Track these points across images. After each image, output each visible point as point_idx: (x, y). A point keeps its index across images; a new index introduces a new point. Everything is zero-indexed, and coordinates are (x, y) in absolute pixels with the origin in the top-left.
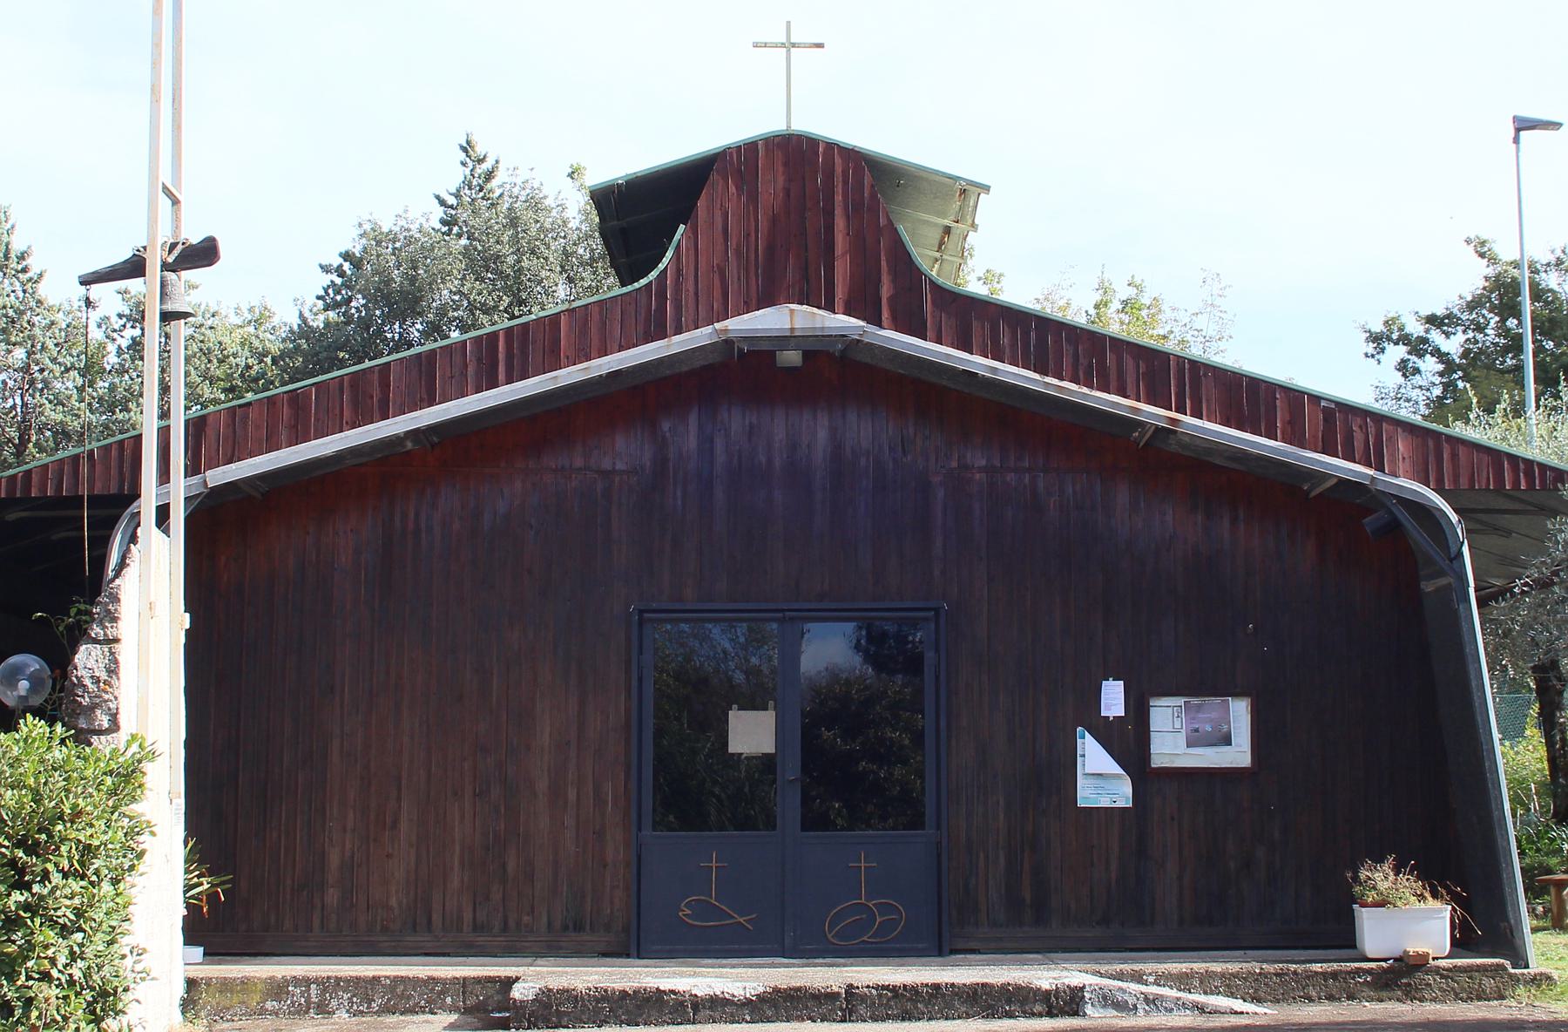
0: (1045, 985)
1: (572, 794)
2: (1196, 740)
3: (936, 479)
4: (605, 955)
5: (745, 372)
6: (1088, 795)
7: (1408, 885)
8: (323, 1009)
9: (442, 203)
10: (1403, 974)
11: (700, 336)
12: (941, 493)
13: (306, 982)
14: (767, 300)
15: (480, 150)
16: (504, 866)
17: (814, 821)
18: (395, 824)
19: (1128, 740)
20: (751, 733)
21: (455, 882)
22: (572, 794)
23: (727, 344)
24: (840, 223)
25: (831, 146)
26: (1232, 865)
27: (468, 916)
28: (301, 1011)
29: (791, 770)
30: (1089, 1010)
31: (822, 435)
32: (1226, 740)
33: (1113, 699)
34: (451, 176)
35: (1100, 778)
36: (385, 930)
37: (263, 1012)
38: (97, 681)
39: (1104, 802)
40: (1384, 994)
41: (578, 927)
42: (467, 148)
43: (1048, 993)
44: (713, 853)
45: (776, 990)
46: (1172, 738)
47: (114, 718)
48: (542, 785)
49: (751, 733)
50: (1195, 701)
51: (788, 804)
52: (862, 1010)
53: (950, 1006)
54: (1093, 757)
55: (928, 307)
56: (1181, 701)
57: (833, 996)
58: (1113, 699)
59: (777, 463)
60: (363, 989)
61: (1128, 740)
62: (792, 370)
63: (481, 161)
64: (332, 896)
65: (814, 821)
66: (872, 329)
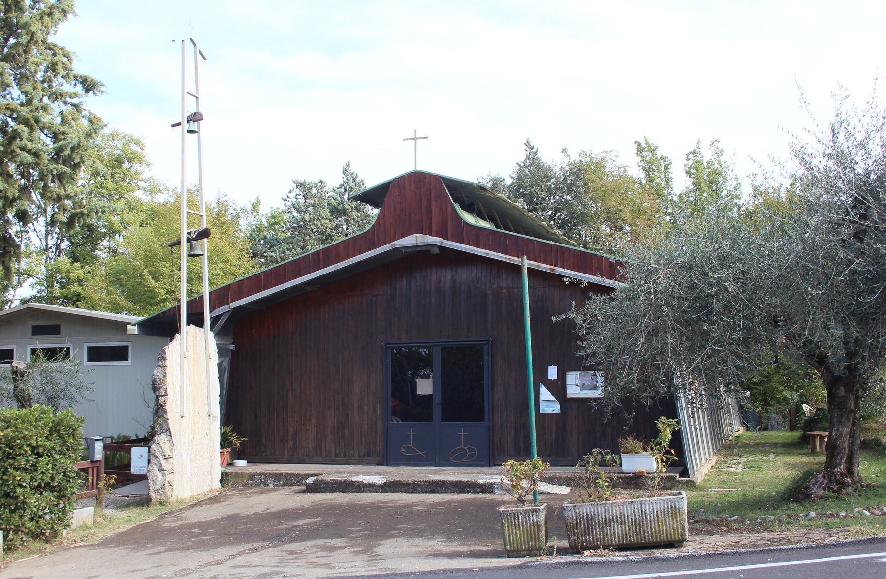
0: (482, 481)
1: (366, 409)
2: (583, 387)
3: (489, 292)
4: (378, 465)
5: (421, 258)
6: (545, 409)
7: (639, 444)
8: (266, 484)
9: (519, 165)
10: (635, 481)
11: (386, 248)
12: (490, 298)
13: (260, 474)
14: (403, 236)
15: (532, 144)
16: (344, 434)
17: (444, 419)
18: (310, 419)
19: (558, 389)
20: (425, 387)
21: (329, 439)
22: (366, 409)
23: (397, 250)
24: (433, 203)
25: (431, 175)
26: (598, 435)
27: (333, 451)
28: (259, 484)
29: (437, 400)
30: (497, 491)
31: (449, 278)
32: (595, 387)
33: (553, 372)
34: (521, 155)
35: (548, 402)
36: (307, 455)
37: (248, 484)
38: (160, 379)
39: (550, 411)
40: (626, 486)
41: (369, 455)
42: (527, 143)
43: (482, 484)
44: (412, 430)
45: (391, 482)
46: (576, 386)
47: (166, 391)
48: (356, 406)
49: (425, 387)
50: (584, 373)
51: (437, 411)
52: (418, 489)
53: (448, 488)
54: (545, 394)
55: (464, 232)
56: (578, 373)
57: (408, 484)
58: (553, 372)
59: (433, 289)
60: (278, 476)
61: (558, 389)
62: (437, 255)
63: (532, 148)
64: (290, 443)
65: (444, 419)
66: (445, 241)
